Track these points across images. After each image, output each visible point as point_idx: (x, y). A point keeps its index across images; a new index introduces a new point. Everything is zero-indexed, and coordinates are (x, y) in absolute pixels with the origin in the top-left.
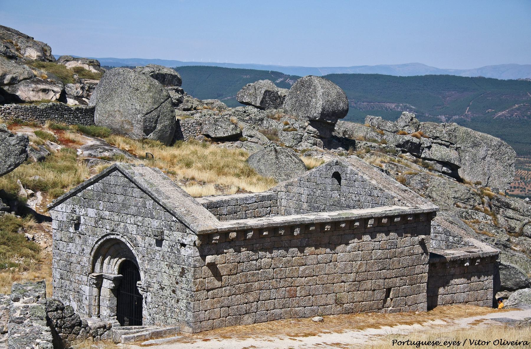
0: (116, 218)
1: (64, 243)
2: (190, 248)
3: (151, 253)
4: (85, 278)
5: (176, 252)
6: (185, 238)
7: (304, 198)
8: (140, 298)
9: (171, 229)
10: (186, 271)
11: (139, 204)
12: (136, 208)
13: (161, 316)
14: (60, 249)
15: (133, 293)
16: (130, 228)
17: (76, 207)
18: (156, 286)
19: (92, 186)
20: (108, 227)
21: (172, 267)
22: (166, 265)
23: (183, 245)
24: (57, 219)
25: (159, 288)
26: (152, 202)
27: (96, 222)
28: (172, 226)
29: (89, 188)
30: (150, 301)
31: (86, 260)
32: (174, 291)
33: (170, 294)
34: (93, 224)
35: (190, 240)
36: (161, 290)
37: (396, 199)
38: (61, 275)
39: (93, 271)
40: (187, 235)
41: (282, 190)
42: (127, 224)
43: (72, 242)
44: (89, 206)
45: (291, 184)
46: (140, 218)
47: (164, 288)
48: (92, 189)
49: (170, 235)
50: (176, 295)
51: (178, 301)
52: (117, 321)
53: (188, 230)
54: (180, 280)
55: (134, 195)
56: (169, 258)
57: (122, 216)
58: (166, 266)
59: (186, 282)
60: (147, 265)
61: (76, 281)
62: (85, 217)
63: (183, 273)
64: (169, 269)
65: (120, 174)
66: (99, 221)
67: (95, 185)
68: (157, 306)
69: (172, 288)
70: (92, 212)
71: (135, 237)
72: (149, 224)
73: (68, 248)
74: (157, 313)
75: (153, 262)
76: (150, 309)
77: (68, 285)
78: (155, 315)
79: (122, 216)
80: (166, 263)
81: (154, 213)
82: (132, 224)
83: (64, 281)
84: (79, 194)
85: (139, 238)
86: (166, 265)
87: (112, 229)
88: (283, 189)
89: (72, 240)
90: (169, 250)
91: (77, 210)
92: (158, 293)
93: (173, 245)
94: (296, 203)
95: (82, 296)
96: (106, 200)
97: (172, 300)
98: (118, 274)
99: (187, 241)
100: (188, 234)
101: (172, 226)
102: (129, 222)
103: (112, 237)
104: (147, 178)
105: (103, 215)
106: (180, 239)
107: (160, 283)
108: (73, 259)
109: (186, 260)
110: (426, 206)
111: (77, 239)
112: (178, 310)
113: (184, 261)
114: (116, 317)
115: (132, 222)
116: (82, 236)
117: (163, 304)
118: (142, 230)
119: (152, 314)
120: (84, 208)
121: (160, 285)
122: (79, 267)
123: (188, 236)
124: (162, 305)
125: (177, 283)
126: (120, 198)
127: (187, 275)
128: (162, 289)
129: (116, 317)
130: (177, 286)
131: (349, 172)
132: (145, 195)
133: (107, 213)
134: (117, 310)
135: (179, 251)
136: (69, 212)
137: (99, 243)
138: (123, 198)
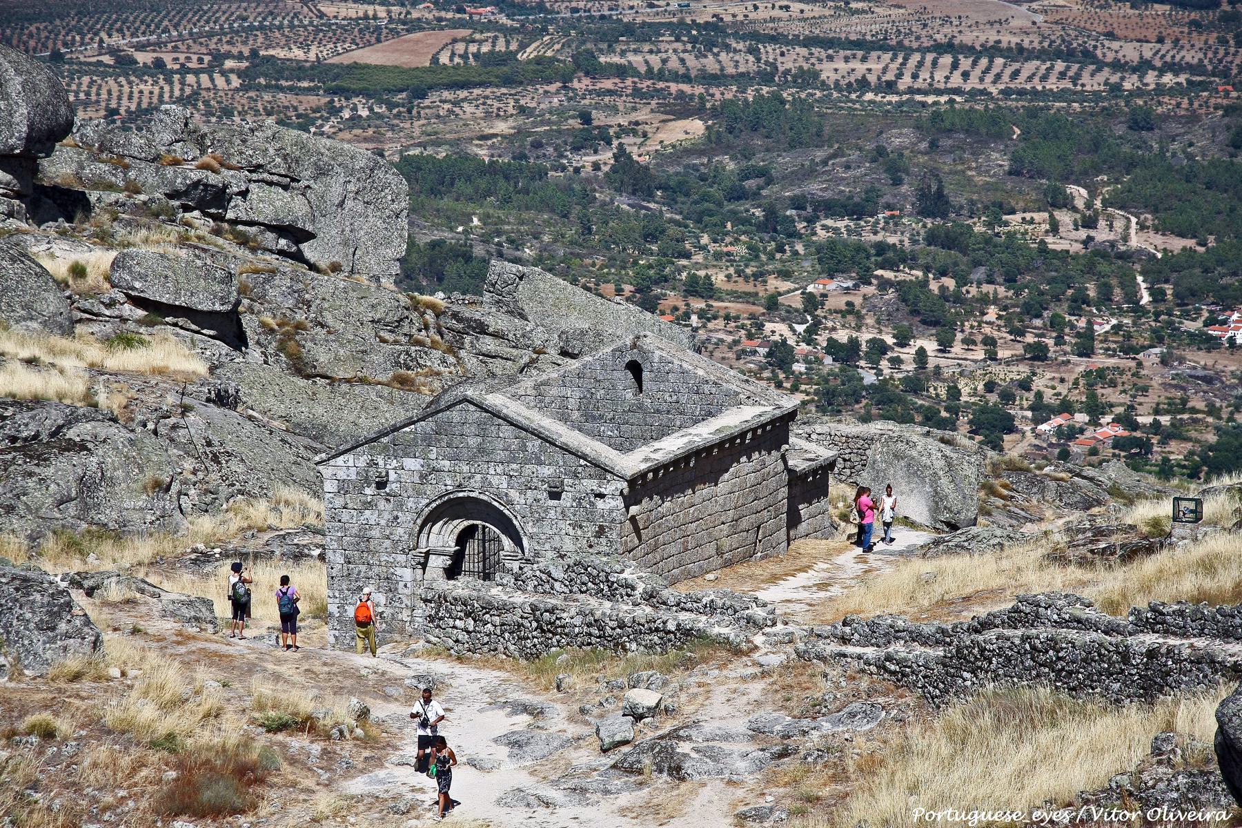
0: (466, 468)
4: (401, 558)
12: (507, 453)
16: (495, 481)
21: (581, 527)
23: (601, 496)
29: (407, 429)
34: (417, 480)
46: (514, 466)
53: (609, 476)
65: (472, 408)
67: (418, 424)
84: (385, 440)
91: (381, 463)
95: (397, 583)
103: (461, 495)
108: (375, 533)
116: (392, 499)
128: (562, 557)
133: (447, 463)
137: (434, 505)
138: (479, 440)
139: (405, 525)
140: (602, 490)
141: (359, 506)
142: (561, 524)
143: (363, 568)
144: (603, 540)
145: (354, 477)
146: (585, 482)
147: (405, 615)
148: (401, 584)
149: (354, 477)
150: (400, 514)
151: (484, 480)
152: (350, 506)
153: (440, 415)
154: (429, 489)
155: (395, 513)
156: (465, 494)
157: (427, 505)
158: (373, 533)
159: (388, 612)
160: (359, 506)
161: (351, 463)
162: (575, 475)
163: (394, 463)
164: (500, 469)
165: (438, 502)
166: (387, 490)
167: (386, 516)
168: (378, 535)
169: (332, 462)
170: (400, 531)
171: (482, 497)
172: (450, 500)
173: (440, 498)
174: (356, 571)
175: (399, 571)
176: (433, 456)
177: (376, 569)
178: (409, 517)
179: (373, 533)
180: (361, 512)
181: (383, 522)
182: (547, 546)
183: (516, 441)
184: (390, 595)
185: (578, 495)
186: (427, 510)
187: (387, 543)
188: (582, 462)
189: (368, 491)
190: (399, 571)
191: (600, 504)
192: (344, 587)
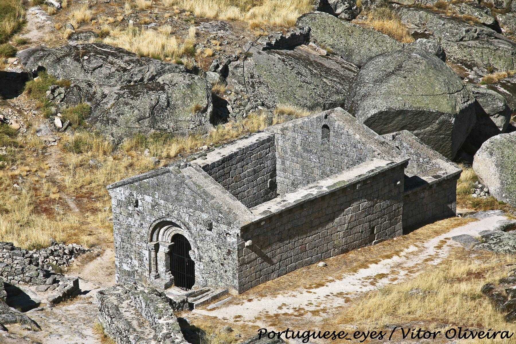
7: (298, 141)
8: (192, 264)
15: (184, 256)
16: (183, 215)
18: (207, 259)
19: (148, 180)
20: (164, 212)
21: (220, 248)
27: (153, 206)
29: (145, 180)
31: (145, 231)
32: (222, 264)
37: (376, 153)
38: (122, 239)
39: (151, 240)
41: (279, 132)
44: (146, 194)
45: (286, 129)
46: (191, 210)
47: (214, 261)
51: (226, 271)
52: (171, 275)
56: (217, 242)
58: (215, 247)
63: (229, 253)
70: (148, 199)
72: (199, 216)
73: (128, 221)
77: (129, 247)
78: (207, 278)
80: (215, 245)
81: (203, 209)
83: (125, 244)
84: (136, 184)
85: (191, 224)
88: (279, 132)
89: (130, 215)
90: (217, 236)
91: (135, 195)
94: (291, 145)
95: (143, 257)
98: (171, 242)
104: (194, 179)
108: (133, 230)
110: (399, 160)
111: (136, 216)
112: (226, 278)
113: (230, 245)
114: (170, 272)
122: (138, 236)
125: (225, 259)
126: (174, 193)
128: (213, 261)
129: (170, 272)
131: (336, 126)
133: (162, 201)
134: (170, 267)
135: (225, 238)
137: (157, 222)
142: (212, 245)
143: (129, 246)
151: (178, 214)
152: (123, 213)
155: (142, 222)
157: (154, 221)
161: (122, 192)
165: (159, 221)
170: (144, 231)
174: (126, 247)
178: (148, 225)
182: (206, 255)
186: (154, 224)
189: (130, 208)
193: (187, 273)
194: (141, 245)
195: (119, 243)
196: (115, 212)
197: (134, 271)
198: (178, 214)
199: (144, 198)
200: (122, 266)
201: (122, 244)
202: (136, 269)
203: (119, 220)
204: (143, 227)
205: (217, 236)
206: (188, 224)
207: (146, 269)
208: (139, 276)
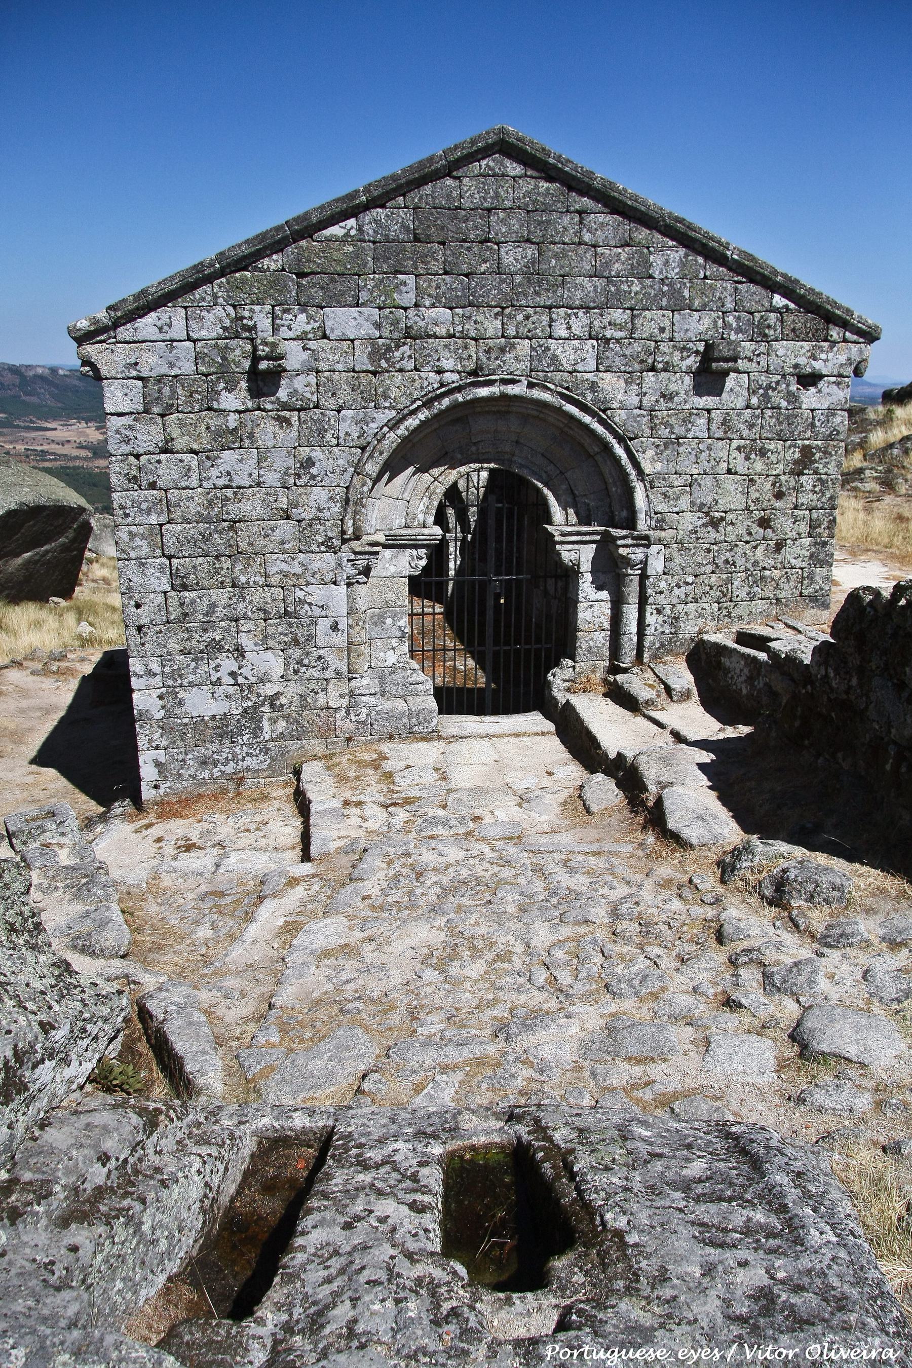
0: (492, 326)
1: (187, 457)
2: (838, 384)
3: (673, 421)
4: (324, 562)
5: (784, 404)
6: (823, 356)
9: (766, 335)
10: (817, 456)
11: (616, 265)
12: (600, 283)
13: (706, 606)
14: (160, 483)
16: (566, 354)
17: (252, 311)
18: (690, 520)
19: (352, 222)
20: (447, 364)
21: (763, 453)
22: (739, 449)
23: (810, 380)
24: (134, 373)
25: (700, 522)
26: (677, 255)
27: (376, 354)
28: (769, 327)
29: (336, 230)
30: (660, 569)
32: (764, 523)
33: (750, 534)
34: (362, 360)
35: (842, 359)
36: (710, 529)
40: (831, 348)
42: (550, 341)
43: (237, 445)
46: (619, 315)
47: (722, 519)
48: (353, 232)
49: (759, 355)
50: (774, 532)
53: (835, 333)
54: (792, 484)
55: (587, 237)
56: (751, 426)
57: (527, 317)
58: (735, 454)
59: (815, 486)
60: (653, 461)
61: (274, 581)
62: (312, 345)
63: (806, 459)
64: (747, 458)
65: (514, 168)
66: (398, 347)
67: (367, 217)
68: (690, 579)
69: (757, 514)
71: (595, 379)
72: (662, 330)
73: (214, 472)
74: (690, 599)
75: (681, 449)
76: (661, 592)
79: (527, 317)
80: (735, 443)
81: (686, 293)
82: (579, 338)
83: (193, 594)
84: (272, 263)
86: (739, 449)
87: (471, 365)
90: (754, 401)
91: (264, 323)
92: (698, 539)
93: (774, 385)
95: (314, 622)
96: (436, 266)
97: (756, 547)
99: (830, 364)
100: (834, 343)
101: (769, 327)
102: (564, 333)
103: (484, 392)
105: (422, 324)
106: (802, 361)
107: (706, 510)
108: (251, 506)
109: (818, 424)
112: (776, 574)
113: (813, 425)
115: (577, 330)
116: (294, 417)
117: (717, 567)
118: (627, 352)
119: (668, 607)
120: (303, 311)
121: (707, 514)
123: (835, 349)
124: (713, 572)
125: (779, 495)
127: (821, 466)
128: (715, 523)
130: (778, 504)
132: (642, 234)
133: (443, 313)
135: (792, 398)
136: (214, 335)
137: (412, 422)
138: (531, 251)
139: (334, 479)
140: (818, 365)
141: (205, 441)
142: (721, 450)
143: (221, 596)
144: (807, 480)
145: (187, 367)
146: (781, 347)
147: (334, 697)
148: (324, 625)
149: (187, 367)
150: (317, 454)
151: (540, 353)
152: (181, 443)
153: (427, 189)
154: (395, 385)
155: (305, 452)
156: (495, 390)
157: (393, 425)
158: (246, 507)
159: (291, 692)
160: (205, 441)
161: (178, 330)
162: (761, 335)
163: (301, 322)
164: (579, 324)
165: (422, 416)
166: (282, 394)
167: (281, 461)
168: (260, 511)
169: (124, 332)
170: (319, 495)
171: (537, 394)
172: (455, 406)
173: (428, 404)
174: (203, 606)
175: (317, 594)
176: (409, 298)
177: (257, 596)
178: (343, 458)
179: (246, 507)
180: (207, 456)
181: (272, 478)
182: (684, 503)
183: (624, 253)
184: (296, 653)
185: (763, 380)
186: (392, 439)
187: (285, 529)
188: (779, 301)
189: (230, 401)
190: (317, 594)
191: (810, 398)
192: (173, 646)
193: (496, 642)
194: (299, 570)
195: (160, 599)
196: (126, 449)
197: (256, 706)
198: (540, 353)
199: (322, 328)
200: (181, 703)
201: (174, 602)
202: (269, 690)
203: (153, 486)
204: (313, 477)
205: (754, 401)
206: (593, 387)
207: (329, 674)
208: (287, 718)
